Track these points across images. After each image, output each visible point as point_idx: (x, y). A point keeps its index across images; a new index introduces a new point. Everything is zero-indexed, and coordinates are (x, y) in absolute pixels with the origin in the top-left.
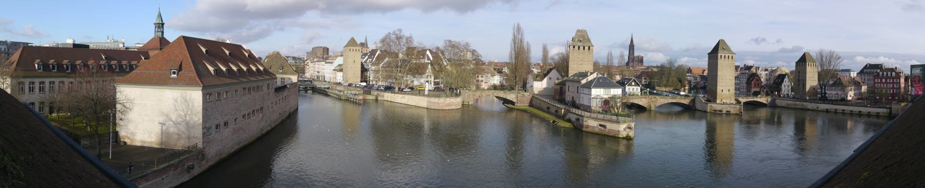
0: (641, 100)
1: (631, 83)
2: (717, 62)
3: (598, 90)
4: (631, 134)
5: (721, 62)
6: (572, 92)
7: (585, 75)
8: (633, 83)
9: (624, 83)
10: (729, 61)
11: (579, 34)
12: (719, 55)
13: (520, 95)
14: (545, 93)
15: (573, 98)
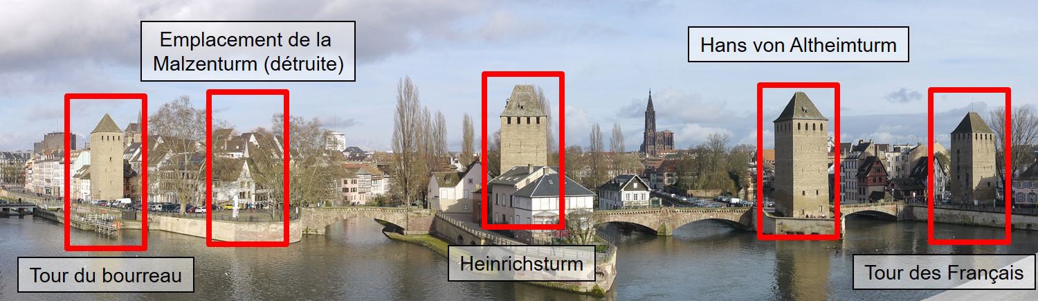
0: (645, 218)
1: (632, 184)
2: (792, 138)
3: (545, 200)
4: (604, 285)
5: (797, 136)
6: (503, 206)
7: (523, 172)
8: (635, 185)
9: (619, 184)
10: (814, 133)
11: (520, 93)
12: (795, 123)
13: (412, 214)
14: (454, 211)
15: (504, 216)
